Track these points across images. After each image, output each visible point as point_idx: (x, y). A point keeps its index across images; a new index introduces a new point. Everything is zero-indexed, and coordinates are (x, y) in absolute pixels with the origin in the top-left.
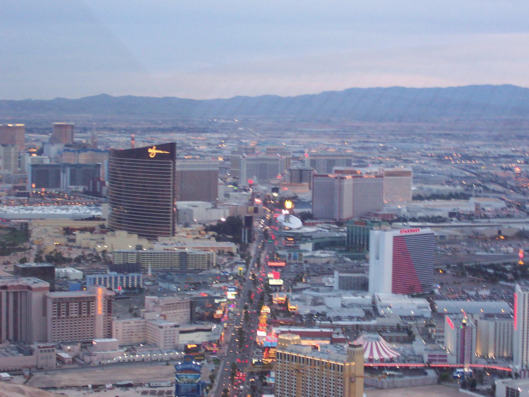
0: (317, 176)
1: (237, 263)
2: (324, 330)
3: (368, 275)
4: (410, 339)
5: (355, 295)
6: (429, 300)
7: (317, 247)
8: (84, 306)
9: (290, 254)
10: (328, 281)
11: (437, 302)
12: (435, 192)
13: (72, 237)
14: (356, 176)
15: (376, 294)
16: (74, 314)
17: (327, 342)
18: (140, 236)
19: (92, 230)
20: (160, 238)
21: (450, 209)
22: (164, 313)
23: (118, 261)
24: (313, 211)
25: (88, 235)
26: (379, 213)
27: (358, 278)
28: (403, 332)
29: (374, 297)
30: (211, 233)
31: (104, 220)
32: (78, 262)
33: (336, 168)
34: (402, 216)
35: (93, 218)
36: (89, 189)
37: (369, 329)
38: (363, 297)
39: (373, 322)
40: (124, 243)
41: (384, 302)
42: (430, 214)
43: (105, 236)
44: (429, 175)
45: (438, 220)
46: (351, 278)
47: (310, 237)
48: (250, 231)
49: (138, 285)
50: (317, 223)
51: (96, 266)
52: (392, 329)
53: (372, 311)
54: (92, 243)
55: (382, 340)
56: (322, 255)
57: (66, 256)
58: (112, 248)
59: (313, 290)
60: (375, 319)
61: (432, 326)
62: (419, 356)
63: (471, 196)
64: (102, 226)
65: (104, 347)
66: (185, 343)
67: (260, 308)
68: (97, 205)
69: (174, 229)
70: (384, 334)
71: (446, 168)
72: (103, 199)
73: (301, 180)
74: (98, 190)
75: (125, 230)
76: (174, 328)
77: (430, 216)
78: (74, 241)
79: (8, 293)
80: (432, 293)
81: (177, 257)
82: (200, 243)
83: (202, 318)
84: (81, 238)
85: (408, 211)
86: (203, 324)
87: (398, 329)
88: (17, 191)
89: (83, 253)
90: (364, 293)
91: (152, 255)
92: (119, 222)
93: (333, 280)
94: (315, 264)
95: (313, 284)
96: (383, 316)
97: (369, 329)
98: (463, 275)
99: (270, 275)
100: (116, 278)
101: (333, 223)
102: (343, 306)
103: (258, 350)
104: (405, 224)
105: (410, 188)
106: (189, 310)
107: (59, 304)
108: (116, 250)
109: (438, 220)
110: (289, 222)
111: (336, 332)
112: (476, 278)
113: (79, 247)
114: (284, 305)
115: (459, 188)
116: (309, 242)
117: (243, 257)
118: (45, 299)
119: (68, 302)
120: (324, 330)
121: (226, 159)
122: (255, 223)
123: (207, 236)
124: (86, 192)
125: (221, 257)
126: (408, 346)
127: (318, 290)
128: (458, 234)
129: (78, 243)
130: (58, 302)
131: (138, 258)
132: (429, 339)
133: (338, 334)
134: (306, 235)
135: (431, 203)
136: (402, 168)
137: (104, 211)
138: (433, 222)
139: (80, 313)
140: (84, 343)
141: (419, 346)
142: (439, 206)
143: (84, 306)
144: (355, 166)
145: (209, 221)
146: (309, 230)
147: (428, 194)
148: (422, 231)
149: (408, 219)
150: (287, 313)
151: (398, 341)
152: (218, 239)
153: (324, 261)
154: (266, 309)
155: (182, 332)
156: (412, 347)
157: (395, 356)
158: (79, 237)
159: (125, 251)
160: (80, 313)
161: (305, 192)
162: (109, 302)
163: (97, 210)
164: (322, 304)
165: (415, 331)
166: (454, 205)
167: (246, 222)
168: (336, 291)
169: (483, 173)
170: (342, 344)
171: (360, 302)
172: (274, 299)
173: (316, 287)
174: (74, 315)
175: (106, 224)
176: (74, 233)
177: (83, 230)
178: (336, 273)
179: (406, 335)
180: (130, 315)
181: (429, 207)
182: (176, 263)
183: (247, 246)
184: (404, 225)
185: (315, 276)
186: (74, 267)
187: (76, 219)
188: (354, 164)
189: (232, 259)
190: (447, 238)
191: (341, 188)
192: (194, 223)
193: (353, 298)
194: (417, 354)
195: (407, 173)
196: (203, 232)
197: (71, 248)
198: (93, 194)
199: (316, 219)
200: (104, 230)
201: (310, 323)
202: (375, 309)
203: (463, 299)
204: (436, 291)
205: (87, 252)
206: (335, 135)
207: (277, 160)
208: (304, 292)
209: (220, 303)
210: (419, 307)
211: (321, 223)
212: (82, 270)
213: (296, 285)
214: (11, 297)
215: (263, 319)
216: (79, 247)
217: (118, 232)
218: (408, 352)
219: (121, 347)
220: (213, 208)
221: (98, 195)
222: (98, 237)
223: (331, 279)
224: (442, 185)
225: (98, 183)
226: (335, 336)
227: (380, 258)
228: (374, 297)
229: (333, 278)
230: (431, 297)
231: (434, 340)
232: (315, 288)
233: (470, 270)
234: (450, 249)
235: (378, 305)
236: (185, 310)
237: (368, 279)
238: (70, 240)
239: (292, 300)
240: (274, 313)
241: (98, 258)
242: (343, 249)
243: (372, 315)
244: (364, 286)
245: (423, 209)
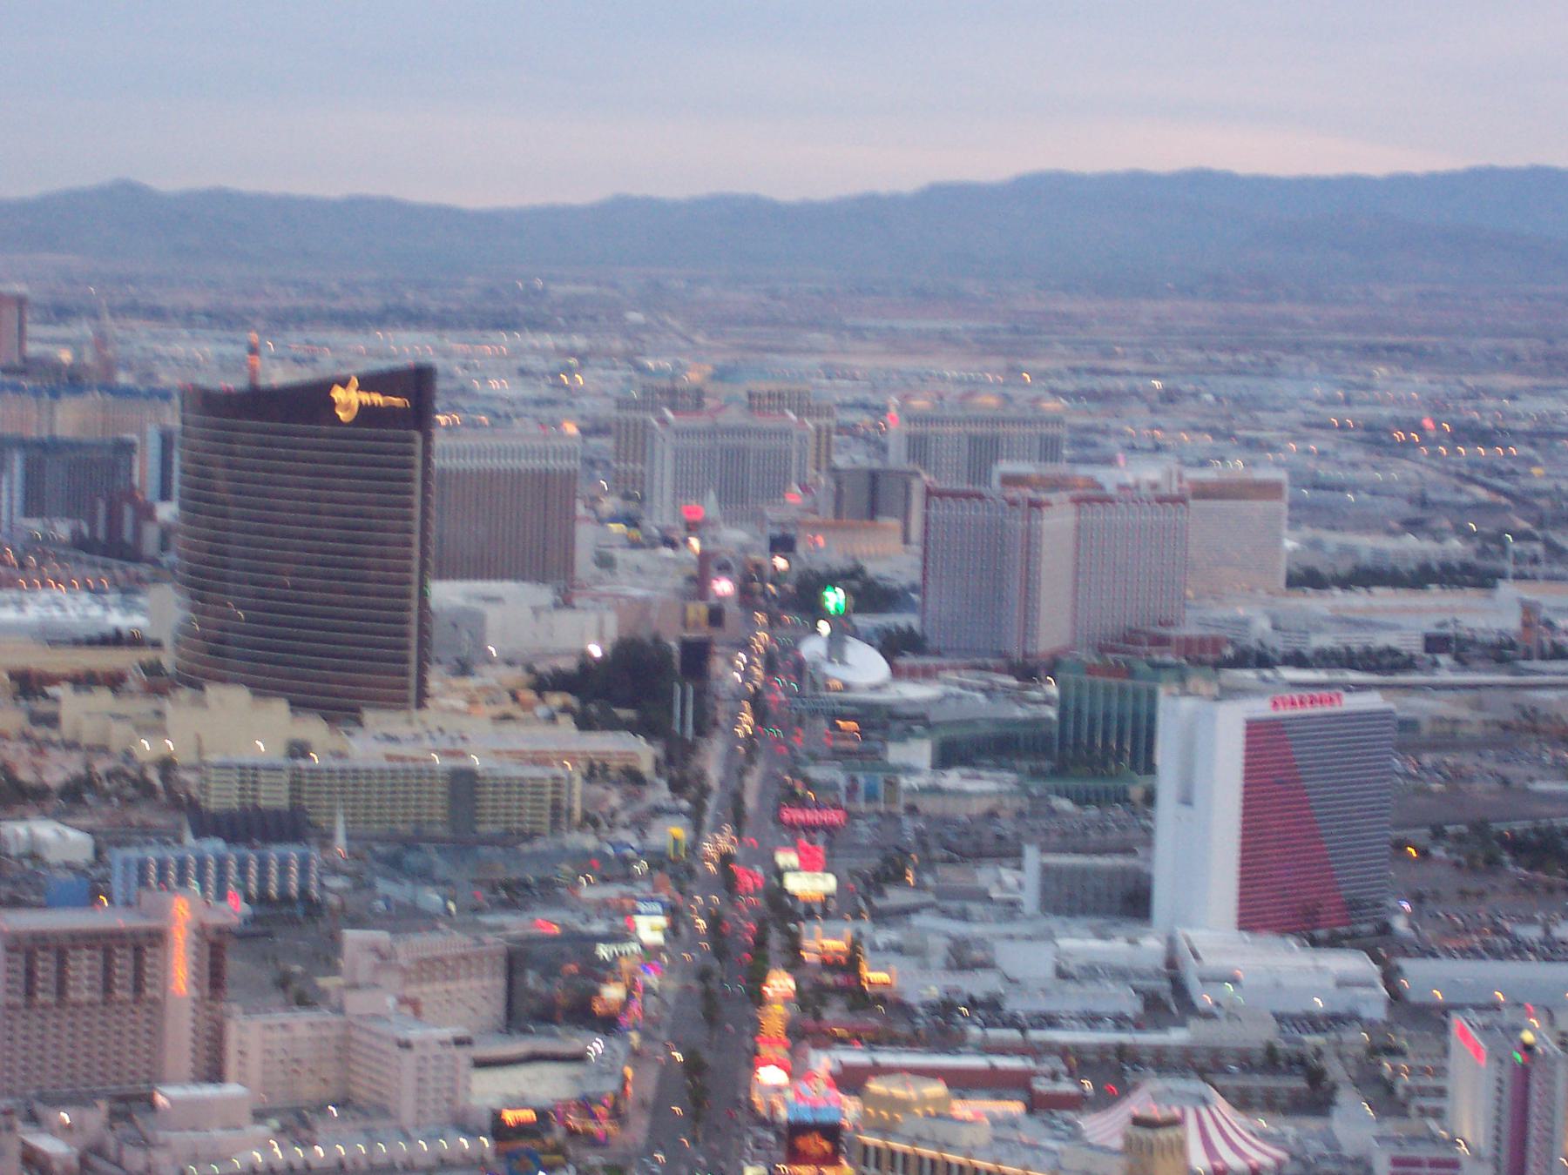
1: (658, 811)
2: (1003, 1062)
3: (1148, 860)
4: (1316, 1099)
5: (1101, 936)
6: (1376, 959)
7: (947, 756)
8: (123, 965)
9: (853, 780)
10: (1000, 882)
11: (1405, 964)
12: (1366, 558)
13: (43, 706)
14: (1092, 498)
15: (1181, 932)
16: (83, 988)
17: (1015, 1108)
18: (297, 706)
19: (115, 682)
20: (369, 716)
21: (1428, 624)
22: (412, 991)
23: (221, 798)
24: (923, 622)
25: (103, 699)
26: (1173, 632)
27: (1112, 874)
28: (1290, 1072)
29: (1171, 942)
30: (556, 699)
31: (157, 644)
32: (72, 797)
33: (1005, 467)
34: (1254, 645)
35: (116, 640)
36: (93, 529)
37: (1162, 1062)
38: (1132, 942)
39: (1176, 1037)
40: (240, 732)
41: (1212, 962)
42: (1357, 641)
43: (167, 706)
44: (1338, 495)
46: (1084, 873)
47: (922, 719)
48: (700, 695)
49: (304, 891)
50: (941, 668)
51: (137, 815)
52: (1247, 1063)
53: (1168, 996)
55: (1221, 1105)
56: (971, 786)
57: (25, 775)
58: (200, 751)
59: (945, 913)
60: (1182, 1024)
61: (1393, 1051)
63: (1502, 575)
64: (153, 670)
65: (194, 1117)
66: (494, 1102)
67: (757, 979)
68: (129, 590)
69: (422, 682)
70: (1221, 1081)
71: (1402, 473)
72: (144, 570)
73: (873, 511)
74: (127, 535)
75: (237, 681)
76: (454, 1050)
77: (1356, 647)
78: (52, 721)
80: (1385, 929)
81: (440, 787)
82: (522, 737)
83: (547, 1016)
84: (79, 711)
85: (1275, 627)
86: (552, 1035)
87: (1272, 1061)
89: (88, 766)
90: (1135, 928)
91: (351, 780)
92: (216, 657)
93: (1020, 881)
94: (945, 821)
95: (942, 893)
96: (1208, 1016)
97: (1162, 1062)
98: (1493, 862)
99: (786, 858)
100: (221, 863)
101: (998, 670)
102: (1062, 974)
103: (761, 1133)
104: (1268, 673)
105: (1278, 540)
106: (500, 982)
107: (30, 957)
108: (214, 758)
109: (1386, 661)
110: (843, 662)
111: (1045, 1067)
112: (1540, 875)
113: (71, 746)
114: (850, 964)
115: (1456, 547)
116: (921, 737)
117: (677, 787)
119: (61, 947)
120: (1003, 1062)
121: (593, 429)
122: (718, 665)
123: (541, 711)
124: (81, 544)
125: (597, 790)
126: (1313, 1124)
127: (964, 916)
128: (1463, 713)
129: (66, 730)
131: (295, 789)
132: (1387, 1100)
133: (1054, 1076)
134: (908, 710)
135: (1356, 600)
136: (1236, 467)
137: (159, 612)
138: (1368, 669)
139: (108, 988)
140: (123, 1099)
141: (1354, 1123)
142: (1386, 610)
143: (123, 965)
145: (544, 655)
146: (914, 692)
147: (1344, 567)
148: (1353, 703)
149: (1278, 659)
150: (861, 999)
151: (1269, 1104)
152: (585, 723)
153: (978, 807)
154: (780, 984)
155: (482, 1064)
156: (1330, 1131)
157: (1267, 1161)
158: (73, 706)
159: (247, 759)
160: (108, 988)
161: (890, 555)
162: (215, 949)
163: (128, 608)
164: (987, 965)
165: (1335, 1070)
166: (1440, 610)
168: (1031, 919)
169: (1539, 494)
170: (1069, 1115)
171: (1122, 962)
172: (807, 943)
173: (956, 903)
174: (85, 996)
175: (168, 659)
176: (51, 690)
177: (85, 681)
178: (1032, 856)
179: (1299, 1083)
180: (278, 997)
181: (1350, 615)
182: (436, 810)
183: (690, 749)
184: (1265, 680)
185: (951, 861)
186: (58, 816)
187: (54, 638)
189: (638, 797)
190: (1426, 729)
191: (1030, 543)
192: (489, 660)
193: (1095, 944)
194: (1348, 1151)
195: (1269, 490)
196: (528, 696)
197: (40, 748)
198: (111, 551)
199: (938, 653)
200: (158, 682)
201: (947, 1040)
202: (1179, 988)
203: (1498, 955)
204: (1400, 924)
205: (101, 766)
206: (986, 344)
207: (786, 433)
208: (917, 920)
210: (1343, 983)
211: (954, 668)
212: (90, 831)
213: (881, 893)
215: (775, 1017)
216: (71, 746)
217: (213, 692)
218: (1316, 1146)
219: (260, 1116)
220: (556, 606)
221: (131, 554)
222: (140, 706)
223: (1009, 876)
224: (1391, 533)
225: (128, 512)
226: (1042, 1086)
227: (1198, 798)
228: (1171, 942)
229: (1019, 868)
230: (1381, 945)
231: (1404, 1105)
232: (954, 905)
233: (1517, 846)
234: (1436, 768)
235: (1191, 973)
236: (487, 982)
237: (1149, 878)
238: (37, 719)
239: (874, 948)
240: (810, 998)
241: (147, 789)
242: (1046, 765)
243: (1167, 1008)
244: (1134, 902)
245: (1326, 619)
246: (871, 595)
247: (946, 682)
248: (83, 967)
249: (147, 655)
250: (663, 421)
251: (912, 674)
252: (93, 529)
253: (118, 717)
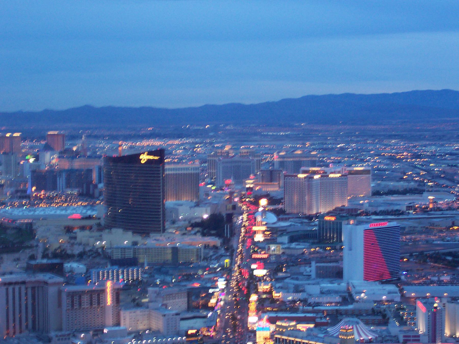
1: (222, 256)
3: (342, 264)
4: (385, 322)
5: (332, 283)
6: (398, 287)
8: (95, 297)
10: (306, 270)
11: (405, 287)
12: (391, 188)
13: (72, 235)
15: (350, 281)
17: (312, 326)
18: (134, 233)
19: (91, 228)
22: (165, 302)
23: (117, 256)
25: (87, 233)
27: (333, 267)
28: (377, 315)
29: (348, 284)
30: (196, 229)
31: (99, 219)
32: (81, 257)
33: (303, 168)
36: (83, 190)
37: (347, 313)
38: (339, 284)
39: (350, 307)
41: (358, 289)
42: (390, 208)
43: (102, 233)
44: (383, 172)
46: (326, 267)
48: (231, 227)
49: (138, 278)
51: (97, 260)
53: (348, 298)
54: (92, 240)
55: (362, 324)
56: (297, 247)
57: (69, 252)
58: (111, 244)
59: (292, 279)
60: (352, 304)
61: (403, 309)
62: (395, 336)
63: (424, 191)
64: (99, 225)
66: (185, 328)
67: (248, 296)
69: (164, 226)
70: (362, 318)
73: (271, 180)
74: (91, 192)
76: (175, 316)
78: (75, 238)
79: (26, 289)
80: (399, 279)
82: (188, 239)
83: (197, 308)
84: (82, 236)
85: (369, 206)
87: (374, 312)
88: (19, 194)
89: (84, 249)
90: (339, 281)
91: (147, 250)
94: (291, 256)
96: (357, 302)
97: (347, 313)
98: (425, 262)
99: (254, 266)
102: (322, 293)
103: (250, 334)
104: (368, 217)
106: (186, 299)
107: (72, 297)
108: (115, 246)
109: (397, 213)
111: (319, 316)
112: (436, 264)
113: (80, 244)
114: (270, 293)
115: (412, 185)
116: (286, 235)
117: (227, 250)
118: (60, 292)
119: (80, 294)
122: (235, 220)
123: (193, 232)
125: (207, 251)
126: (384, 328)
127: (297, 279)
128: (416, 225)
129: (78, 240)
130: (72, 295)
131: (135, 253)
133: (321, 318)
137: (100, 210)
139: (91, 304)
141: (394, 327)
142: (396, 200)
143: (95, 297)
145: (193, 218)
146: (283, 224)
147: (386, 190)
148: (388, 224)
150: (273, 301)
151: (373, 323)
152: (204, 235)
153: (300, 252)
154: (254, 297)
155: (183, 319)
156: (388, 329)
159: (122, 246)
160: (91, 304)
162: (117, 294)
164: (303, 291)
165: (389, 314)
166: (409, 200)
168: (314, 279)
170: (325, 327)
171: (337, 289)
172: (259, 287)
173: (296, 276)
174: (86, 306)
175: (103, 222)
177: (83, 228)
178: (313, 263)
179: (380, 318)
180: (132, 304)
182: (169, 257)
183: (229, 240)
185: (293, 265)
186: (78, 261)
189: (217, 252)
192: (179, 220)
193: (329, 285)
194: (393, 334)
196: (189, 229)
197: (73, 244)
199: (288, 214)
200: (100, 228)
201: (295, 310)
202: (351, 295)
203: (428, 284)
204: (403, 278)
205: (88, 249)
207: (249, 162)
208: (287, 280)
209: (213, 293)
210: (389, 293)
213: (277, 275)
214: (30, 291)
215: (253, 306)
216: (80, 244)
217: (114, 230)
218: (385, 333)
222: (97, 234)
223: (308, 269)
224: (397, 181)
225: (91, 187)
226: (318, 320)
228: (348, 284)
229: (310, 267)
231: (406, 322)
232: (296, 276)
233: (431, 257)
234: (410, 239)
236: (183, 299)
237: (342, 268)
238: (71, 238)
240: (260, 301)
241: (99, 254)
242: (316, 241)
243: (347, 300)
244: (338, 274)
245: (382, 203)
247: (290, 222)
248: (85, 298)
249: (98, 221)
252: (83, 190)
253: (91, 237)
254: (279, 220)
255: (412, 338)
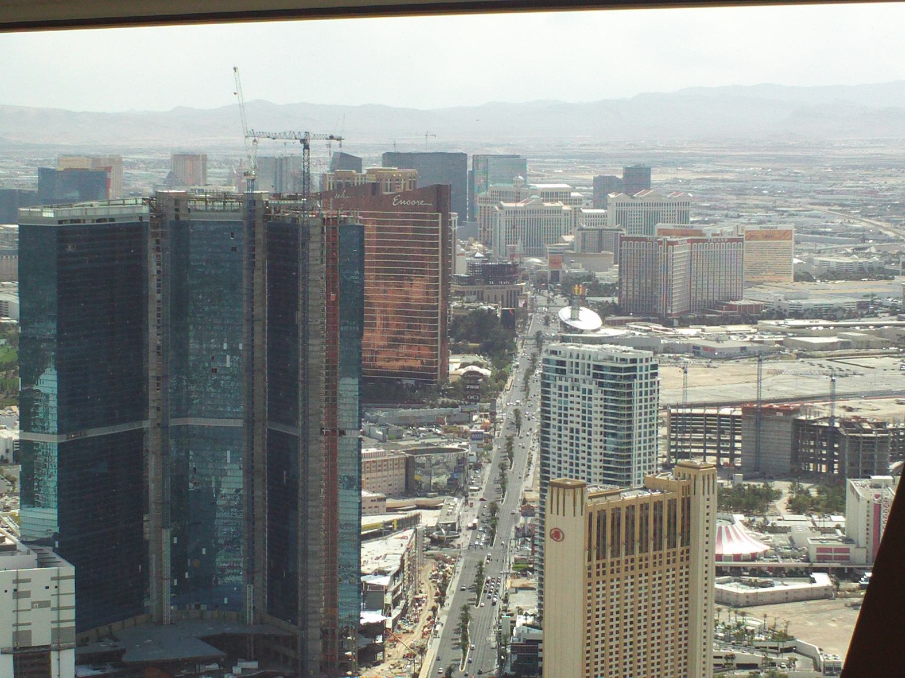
0: (628, 239)
24: (620, 301)
33: (660, 225)
34: (775, 307)
45: (839, 314)
104: (781, 322)
105: (791, 260)
144: (693, 222)
149: (787, 314)
167: (732, 305)
184: (779, 325)
188: (691, 219)
195: (786, 235)
246: (597, 289)
247: (628, 328)
250: (501, 208)
251: (613, 324)
254: (606, 323)
255: (833, 554)
